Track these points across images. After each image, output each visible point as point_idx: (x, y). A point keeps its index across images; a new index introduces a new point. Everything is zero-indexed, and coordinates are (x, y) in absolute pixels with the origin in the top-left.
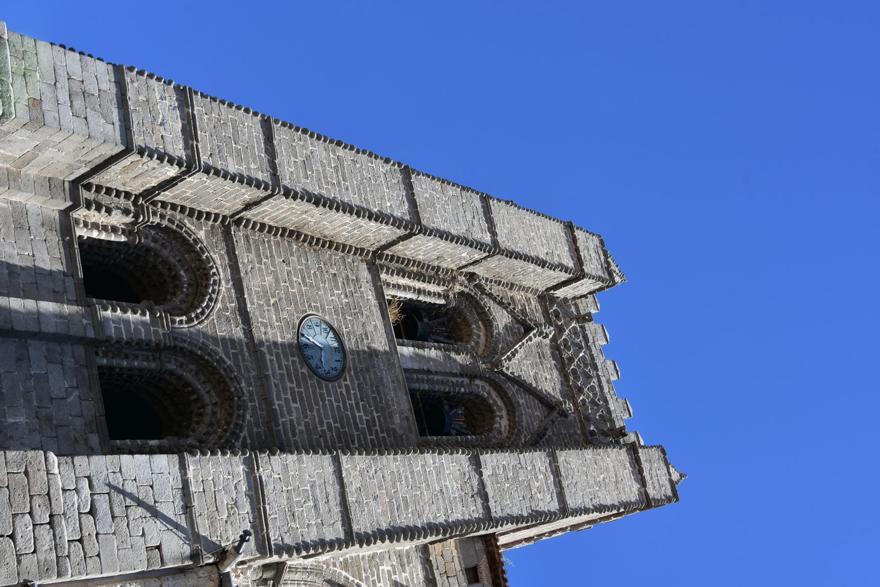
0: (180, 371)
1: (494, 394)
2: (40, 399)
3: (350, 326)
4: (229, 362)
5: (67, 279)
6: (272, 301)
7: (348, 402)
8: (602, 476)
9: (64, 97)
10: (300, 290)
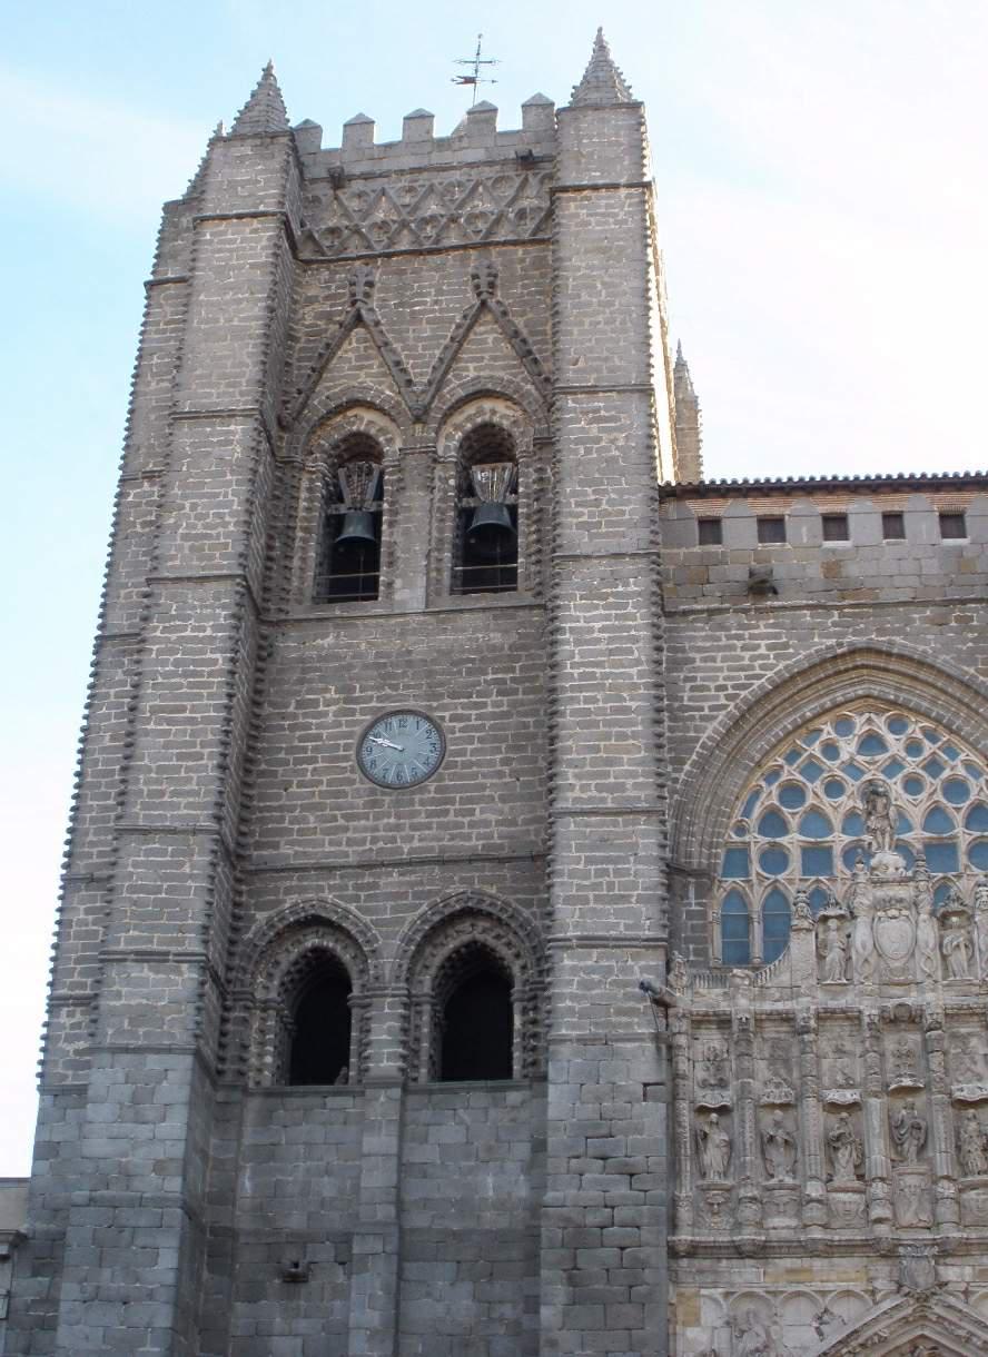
0: (433, 971)
1: (458, 418)
2: (467, 1157)
3: (370, 693)
4: (424, 908)
5: (329, 1105)
6: (341, 822)
7: (473, 722)
8: (599, 286)
9: (144, 1131)
10: (327, 770)
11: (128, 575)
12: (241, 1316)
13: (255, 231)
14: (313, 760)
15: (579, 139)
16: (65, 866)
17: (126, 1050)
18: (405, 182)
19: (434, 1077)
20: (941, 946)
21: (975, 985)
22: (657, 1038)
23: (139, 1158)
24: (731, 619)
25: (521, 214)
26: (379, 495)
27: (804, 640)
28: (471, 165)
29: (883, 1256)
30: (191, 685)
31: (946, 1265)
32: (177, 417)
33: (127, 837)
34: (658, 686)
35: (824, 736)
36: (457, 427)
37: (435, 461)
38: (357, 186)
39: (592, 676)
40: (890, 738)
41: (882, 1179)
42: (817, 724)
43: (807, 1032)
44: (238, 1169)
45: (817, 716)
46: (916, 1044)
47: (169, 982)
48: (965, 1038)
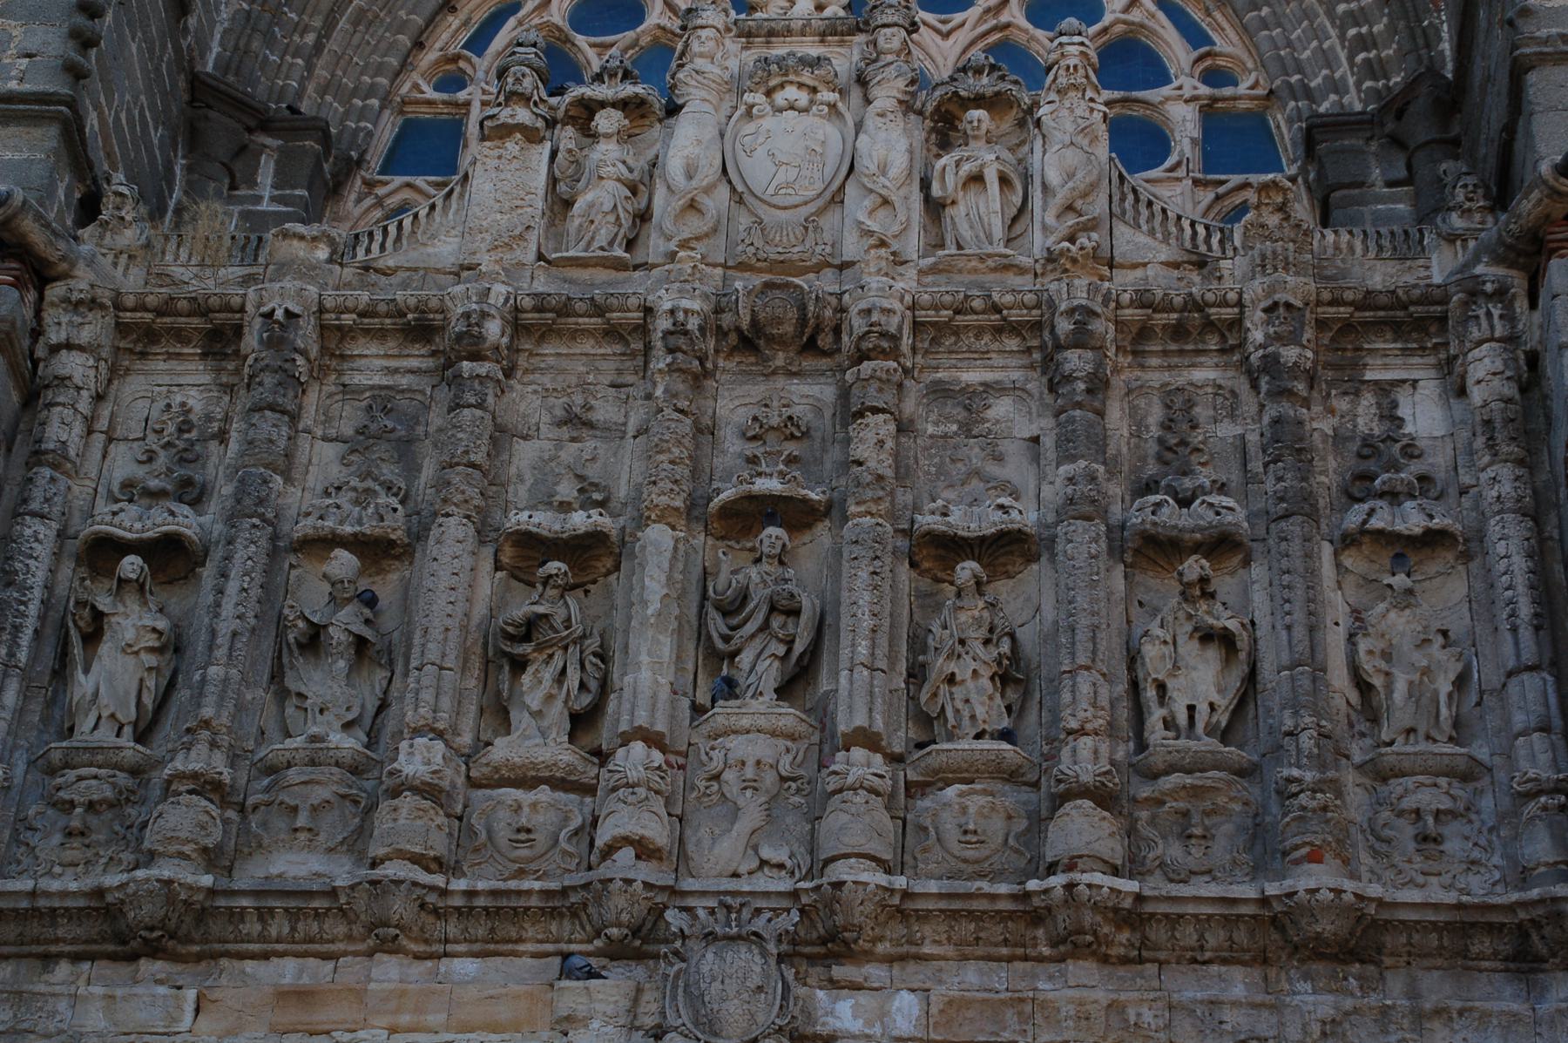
20: (925, 185)
21: (1021, 271)
29: (618, 952)
31: (834, 984)
41: (653, 740)
43: (476, 357)
46: (818, 411)
48: (973, 400)
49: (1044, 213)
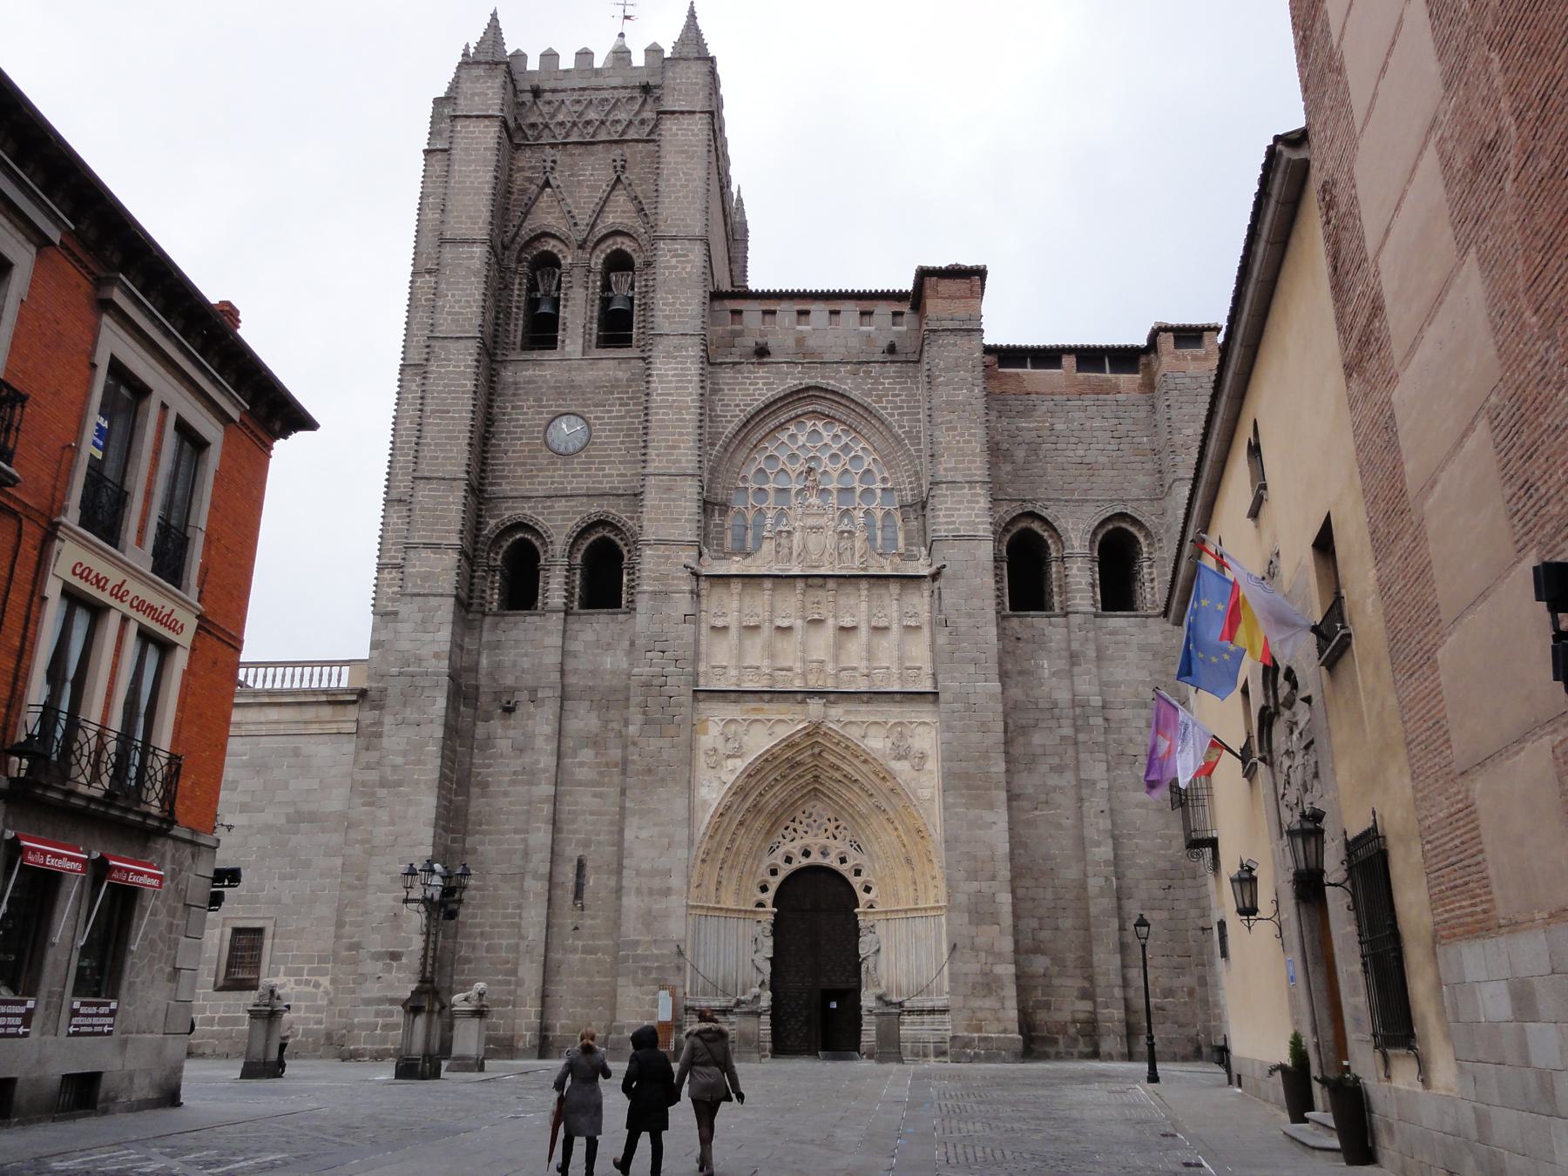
0: (582, 552)
1: (603, 246)
9: (428, 637)
11: (418, 329)
12: (481, 730)
13: (486, 126)
14: (521, 439)
15: (675, 79)
16: (385, 493)
17: (419, 595)
18: (576, 96)
19: (582, 606)
22: (692, 592)
23: (426, 651)
24: (745, 367)
25: (643, 122)
26: (559, 288)
27: (783, 380)
28: (614, 88)
30: (453, 398)
32: (443, 241)
33: (418, 482)
34: (701, 408)
35: (790, 432)
36: (602, 252)
37: (589, 271)
38: (548, 96)
39: (667, 401)
40: (825, 434)
42: (787, 426)
44: (479, 654)
45: (788, 421)
47: (441, 559)
49: (857, 555)
